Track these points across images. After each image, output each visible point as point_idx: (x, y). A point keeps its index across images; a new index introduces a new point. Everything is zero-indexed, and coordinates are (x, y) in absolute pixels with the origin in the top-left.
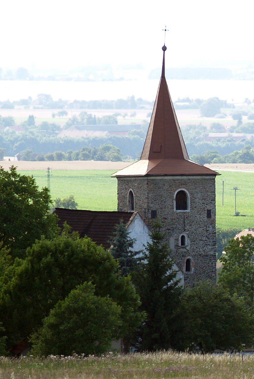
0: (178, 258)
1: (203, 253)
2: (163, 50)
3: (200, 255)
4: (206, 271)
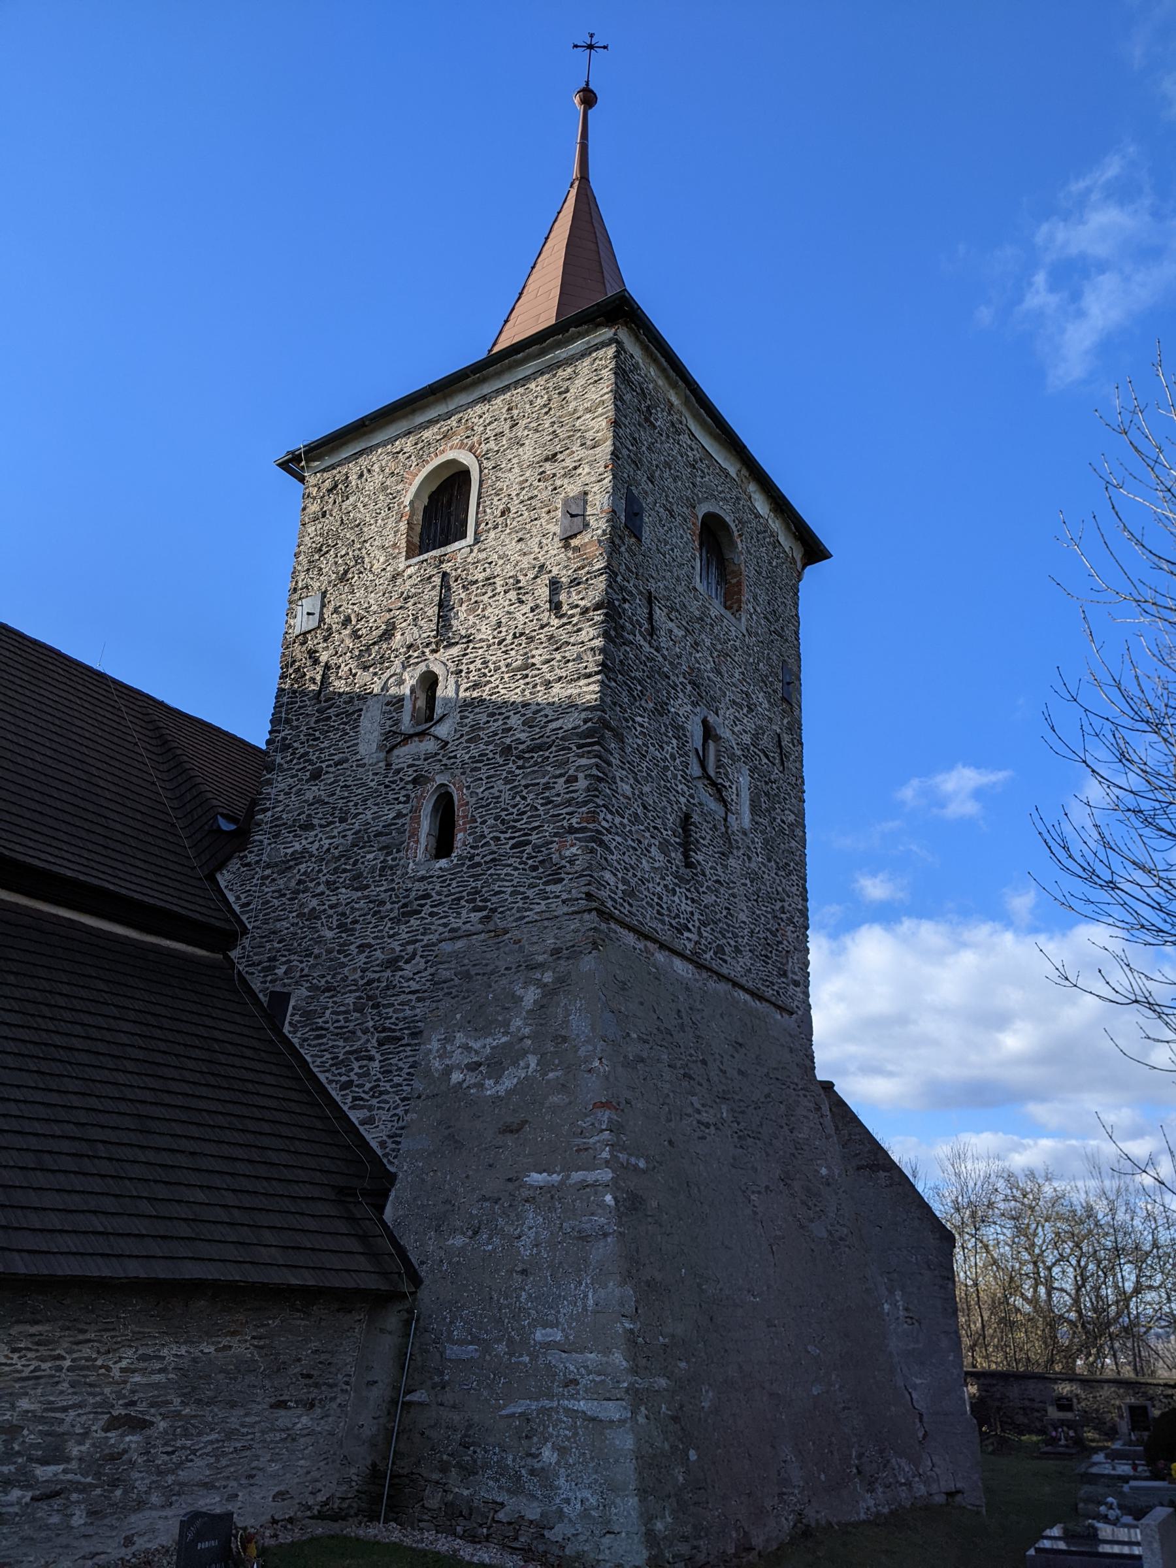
0: (391, 796)
1: (523, 736)
3: (507, 750)
4: (533, 837)
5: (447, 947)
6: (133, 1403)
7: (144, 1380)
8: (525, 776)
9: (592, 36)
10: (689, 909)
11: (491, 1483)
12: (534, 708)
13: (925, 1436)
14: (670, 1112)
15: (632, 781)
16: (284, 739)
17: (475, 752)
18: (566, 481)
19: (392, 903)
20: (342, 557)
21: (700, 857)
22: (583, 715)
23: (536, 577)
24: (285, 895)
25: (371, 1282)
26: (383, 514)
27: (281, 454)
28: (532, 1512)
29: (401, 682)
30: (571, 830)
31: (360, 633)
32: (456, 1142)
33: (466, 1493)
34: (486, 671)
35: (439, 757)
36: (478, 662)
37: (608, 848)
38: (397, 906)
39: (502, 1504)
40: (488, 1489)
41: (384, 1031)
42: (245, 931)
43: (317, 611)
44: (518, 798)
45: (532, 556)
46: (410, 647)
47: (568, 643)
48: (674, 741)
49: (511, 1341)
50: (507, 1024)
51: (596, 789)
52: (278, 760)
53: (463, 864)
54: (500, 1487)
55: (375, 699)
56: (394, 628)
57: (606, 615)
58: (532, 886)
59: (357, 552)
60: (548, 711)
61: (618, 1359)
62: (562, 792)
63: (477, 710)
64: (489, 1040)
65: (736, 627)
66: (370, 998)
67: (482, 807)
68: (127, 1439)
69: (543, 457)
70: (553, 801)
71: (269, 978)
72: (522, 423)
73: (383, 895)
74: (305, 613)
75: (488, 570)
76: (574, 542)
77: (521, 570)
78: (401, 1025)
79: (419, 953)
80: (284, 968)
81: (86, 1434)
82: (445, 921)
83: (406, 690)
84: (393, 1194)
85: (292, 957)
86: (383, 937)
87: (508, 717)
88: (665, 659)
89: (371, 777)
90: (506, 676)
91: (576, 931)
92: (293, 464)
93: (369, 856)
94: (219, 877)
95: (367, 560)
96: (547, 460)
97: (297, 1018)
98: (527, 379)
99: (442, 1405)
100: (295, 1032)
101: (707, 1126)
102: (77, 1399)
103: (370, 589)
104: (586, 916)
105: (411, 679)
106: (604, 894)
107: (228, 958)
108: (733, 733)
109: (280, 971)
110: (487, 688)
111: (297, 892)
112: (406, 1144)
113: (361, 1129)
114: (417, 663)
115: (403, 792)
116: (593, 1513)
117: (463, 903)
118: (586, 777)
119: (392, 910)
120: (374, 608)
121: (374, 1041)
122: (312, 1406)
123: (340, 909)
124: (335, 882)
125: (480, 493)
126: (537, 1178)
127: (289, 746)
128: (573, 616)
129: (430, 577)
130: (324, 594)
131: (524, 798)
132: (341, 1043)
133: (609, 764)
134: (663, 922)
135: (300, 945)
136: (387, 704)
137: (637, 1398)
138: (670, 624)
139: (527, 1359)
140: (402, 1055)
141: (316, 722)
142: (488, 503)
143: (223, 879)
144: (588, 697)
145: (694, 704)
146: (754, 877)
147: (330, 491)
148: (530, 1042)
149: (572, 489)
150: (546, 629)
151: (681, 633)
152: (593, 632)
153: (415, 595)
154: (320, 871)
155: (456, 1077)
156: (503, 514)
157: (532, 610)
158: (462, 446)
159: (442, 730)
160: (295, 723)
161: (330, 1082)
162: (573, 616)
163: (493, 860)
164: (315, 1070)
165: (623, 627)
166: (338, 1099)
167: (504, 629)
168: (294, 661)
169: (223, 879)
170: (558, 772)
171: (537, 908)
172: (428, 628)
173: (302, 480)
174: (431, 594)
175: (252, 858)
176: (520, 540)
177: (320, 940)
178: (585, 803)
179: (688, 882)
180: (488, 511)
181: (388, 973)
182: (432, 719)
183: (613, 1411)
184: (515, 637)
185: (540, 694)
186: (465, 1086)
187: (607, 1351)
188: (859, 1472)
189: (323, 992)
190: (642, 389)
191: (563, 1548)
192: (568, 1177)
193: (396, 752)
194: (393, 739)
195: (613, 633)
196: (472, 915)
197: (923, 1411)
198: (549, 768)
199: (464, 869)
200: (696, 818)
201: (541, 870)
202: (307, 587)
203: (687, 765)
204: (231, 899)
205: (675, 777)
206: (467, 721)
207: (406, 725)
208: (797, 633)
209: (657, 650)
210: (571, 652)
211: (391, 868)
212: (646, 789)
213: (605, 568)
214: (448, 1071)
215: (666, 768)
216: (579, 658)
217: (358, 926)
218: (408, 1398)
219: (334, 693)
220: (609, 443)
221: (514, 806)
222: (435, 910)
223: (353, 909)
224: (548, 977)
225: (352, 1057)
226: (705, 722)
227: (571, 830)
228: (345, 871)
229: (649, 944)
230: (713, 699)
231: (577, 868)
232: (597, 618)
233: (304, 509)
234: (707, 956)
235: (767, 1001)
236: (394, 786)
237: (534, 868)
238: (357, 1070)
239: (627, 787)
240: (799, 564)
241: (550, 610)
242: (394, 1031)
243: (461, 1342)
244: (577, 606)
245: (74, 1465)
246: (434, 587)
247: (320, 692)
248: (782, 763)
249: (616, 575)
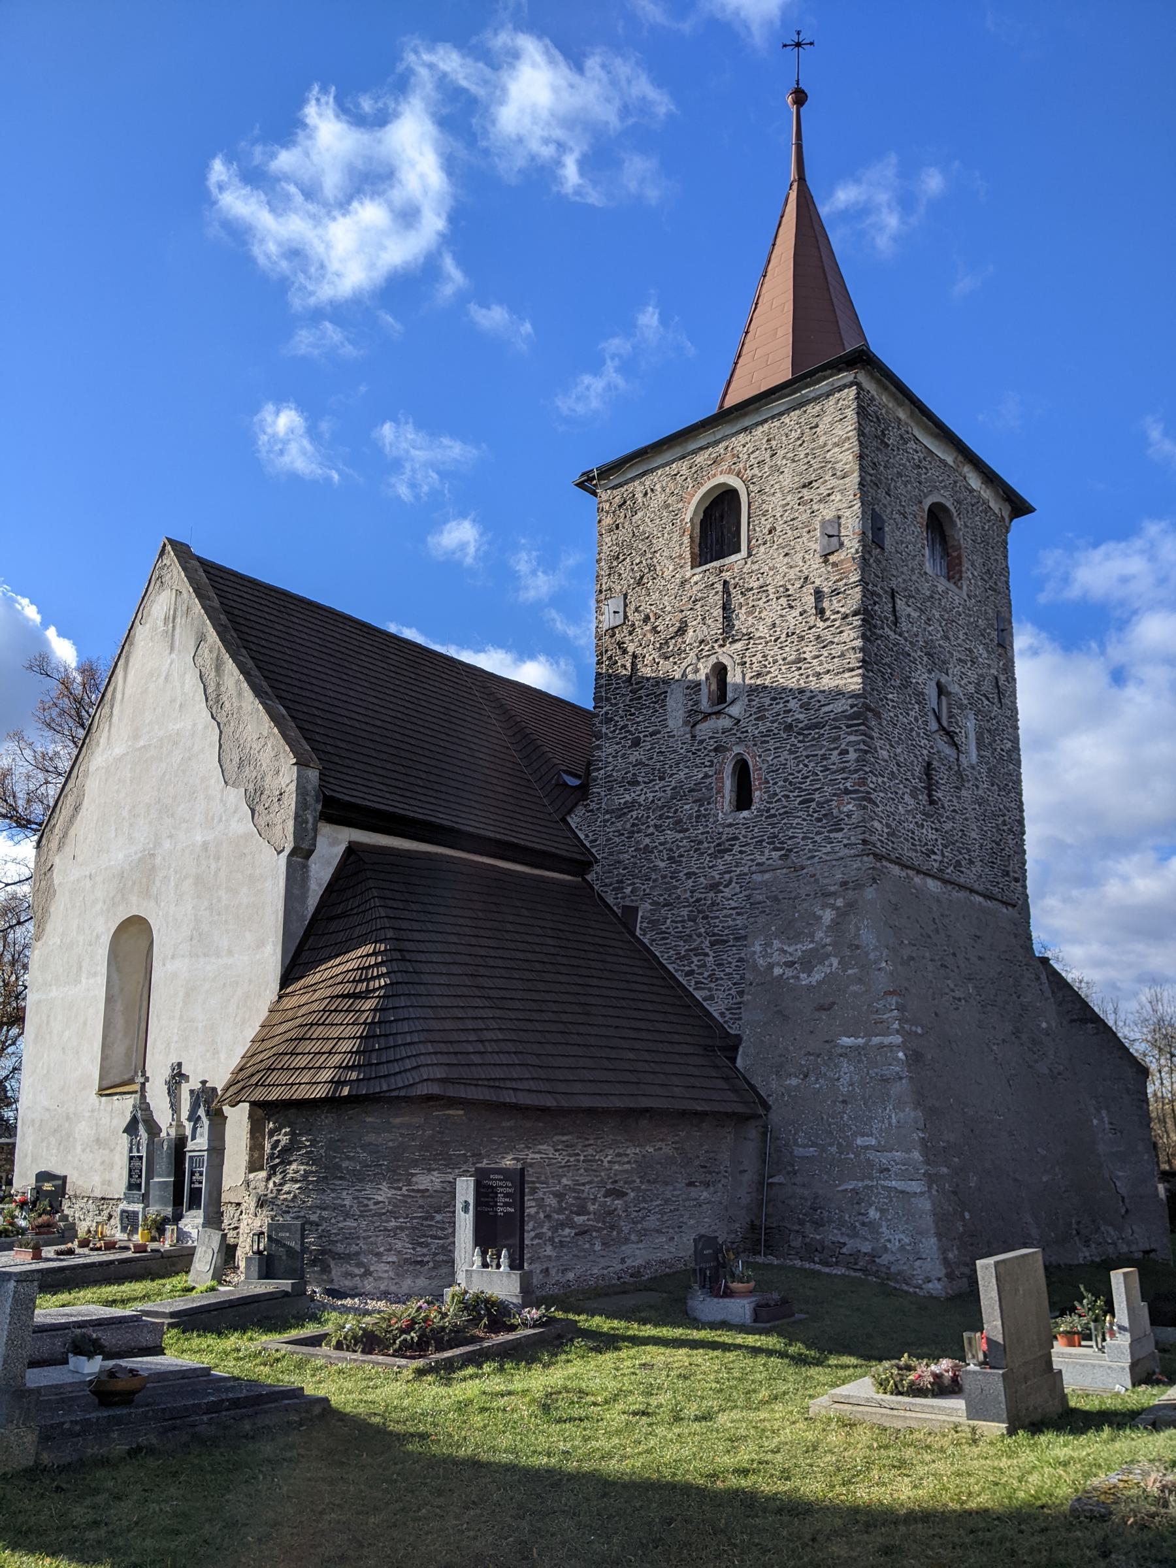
0: (698, 761)
1: (801, 717)
3: (789, 728)
4: (816, 796)
5: (757, 878)
6: (616, 1182)
7: (620, 1168)
8: (806, 748)
9: (798, 33)
10: (934, 837)
11: (835, 1231)
12: (809, 694)
13: (1127, 1211)
14: (934, 993)
15: (888, 747)
16: (607, 713)
17: (762, 729)
18: (822, 506)
19: (709, 843)
20: (637, 564)
21: (940, 795)
22: (850, 701)
23: (802, 587)
24: (623, 834)
25: (740, 1109)
26: (668, 529)
27: (577, 478)
28: (866, 1248)
29: (697, 671)
30: (847, 792)
31: (659, 629)
32: (784, 1015)
33: (818, 1237)
34: (766, 663)
35: (734, 731)
36: (759, 656)
37: (875, 804)
38: (712, 845)
39: (845, 1244)
40: (832, 1235)
41: (714, 935)
42: (597, 861)
43: (621, 610)
44: (801, 766)
45: (798, 569)
46: (702, 642)
47: (832, 643)
48: (917, 706)
49: (840, 1145)
50: (812, 935)
51: (864, 760)
52: (604, 730)
53: (762, 815)
54: (842, 1234)
55: (677, 683)
56: (687, 626)
57: (863, 620)
58: (818, 833)
59: (649, 561)
60: (820, 697)
61: (916, 1155)
62: (837, 761)
63: (761, 695)
64: (799, 946)
65: (957, 596)
66: (699, 912)
67: (773, 771)
68: (616, 1202)
69: (801, 484)
70: (829, 769)
71: (619, 896)
72: (781, 453)
73: (700, 837)
74: (611, 612)
75: (761, 579)
76: (832, 559)
77: (789, 580)
78: (726, 932)
79: (735, 880)
80: (630, 888)
81: (595, 1199)
82: (752, 857)
83: (702, 676)
84: (741, 1050)
85: (636, 881)
86: (704, 868)
87: (788, 701)
88: (906, 640)
89: (680, 746)
90: (783, 668)
91: (859, 869)
92: (587, 483)
93: (686, 807)
94: (569, 819)
95: (658, 568)
96: (804, 486)
97: (645, 925)
98: (781, 414)
99: (795, 1184)
100: (644, 935)
101: (959, 1000)
102: (589, 1179)
103: (664, 593)
104: (865, 858)
105: (704, 669)
106: (874, 838)
107: (585, 880)
108: (961, 686)
109: (628, 890)
110: (768, 677)
111: (633, 832)
113: (705, 1003)
114: (709, 656)
115: (708, 758)
116: (908, 1247)
117: (764, 844)
118: (855, 751)
119: (709, 848)
120: (668, 608)
121: (707, 942)
122: (709, 1185)
123: (668, 846)
124: (661, 826)
125: (749, 514)
126: (846, 1041)
127: (611, 719)
128: (835, 620)
129: (713, 584)
130: (625, 596)
131: (806, 766)
132: (682, 943)
133: (872, 738)
134: (916, 851)
135: (640, 872)
136: (688, 688)
137: (931, 1179)
138: (909, 609)
139: (853, 1156)
140: (730, 953)
141: (630, 700)
142: (757, 522)
143: (573, 821)
144: (853, 687)
145: (930, 672)
146: (981, 801)
147: (620, 506)
148: (831, 948)
149: (828, 513)
150: (813, 630)
151: (915, 614)
152: (853, 635)
153: (702, 599)
154: (648, 817)
155: (777, 971)
156: (770, 532)
157: (801, 614)
158: (730, 471)
159: (735, 710)
160: (614, 701)
161: (677, 971)
162: (835, 620)
163: (786, 812)
164: (664, 962)
165: (875, 627)
166: (684, 982)
167: (778, 629)
168: (606, 651)
169: (573, 821)
170: (832, 746)
171: (824, 850)
172: (716, 628)
173: (595, 494)
174: (716, 599)
175: (593, 806)
176: (786, 555)
177: (655, 869)
178: (856, 771)
179: (932, 816)
180: (758, 529)
181: (712, 894)
182: (726, 702)
183: (916, 1187)
184: (788, 635)
185: (813, 684)
186: (785, 977)
187: (908, 1151)
188: (1078, 1233)
189: (664, 906)
190: (878, 418)
191: (889, 1268)
192: (870, 1040)
193: (698, 727)
194: (694, 717)
195: (868, 633)
196: (773, 853)
197: (1125, 1195)
198: (824, 743)
199: (763, 818)
200: (935, 764)
201: (824, 821)
202: (610, 589)
203: (926, 723)
204: (582, 837)
205: (918, 734)
206: (754, 703)
207: (705, 705)
208: (1007, 583)
209: (900, 636)
210: (836, 650)
211: (705, 816)
212: (899, 750)
213: (859, 581)
214: (771, 966)
215: (912, 730)
216: (843, 655)
217: (684, 859)
218: (770, 1180)
219: (642, 677)
220: (856, 474)
221: (799, 772)
222: (743, 849)
223: (678, 847)
224: (840, 903)
225: (691, 954)
226: (939, 684)
227: (847, 792)
228: (668, 817)
229: (911, 873)
230: (944, 662)
231: (854, 821)
232: (855, 623)
233: (600, 522)
234: (949, 871)
235: (996, 899)
236: (699, 753)
237: (819, 820)
238: (696, 963)
239: (885, 753)
240: (1007, 520)
241: (816, 615)
242: (722, 936)
243: (804, 1146)
244: (838, 612)
245: (592, 1216)
246: (717, 592)
247: (631, 677)
248: (1000, 701)
249: (867, 584)
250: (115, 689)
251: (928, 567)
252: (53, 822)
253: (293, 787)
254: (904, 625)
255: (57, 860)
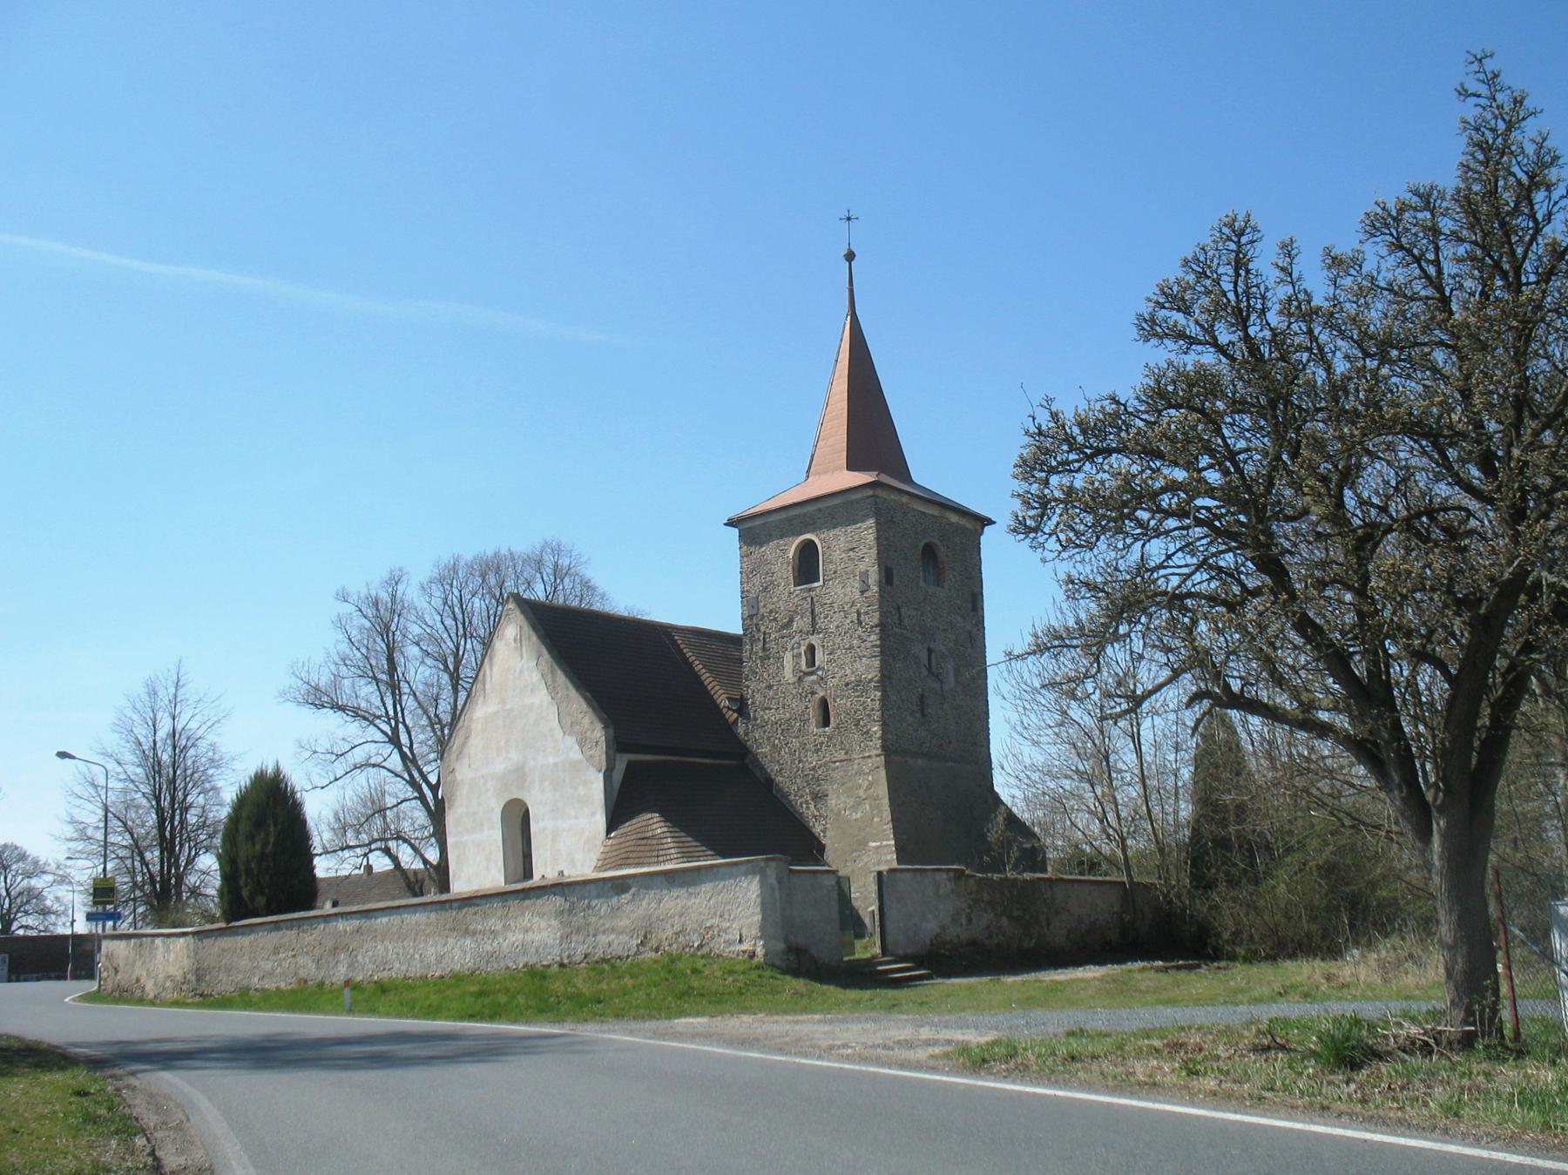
2: (847, 260)
36: (831, 643)
96: (851, 550)
112: (828, 834)
149: (862, 567)
151: (913, 613)
250: (484, 675)
251: (922, 583)
252: (451, 744)
253: (603, 738)
254: (906, 622)
255: (457, 768)
